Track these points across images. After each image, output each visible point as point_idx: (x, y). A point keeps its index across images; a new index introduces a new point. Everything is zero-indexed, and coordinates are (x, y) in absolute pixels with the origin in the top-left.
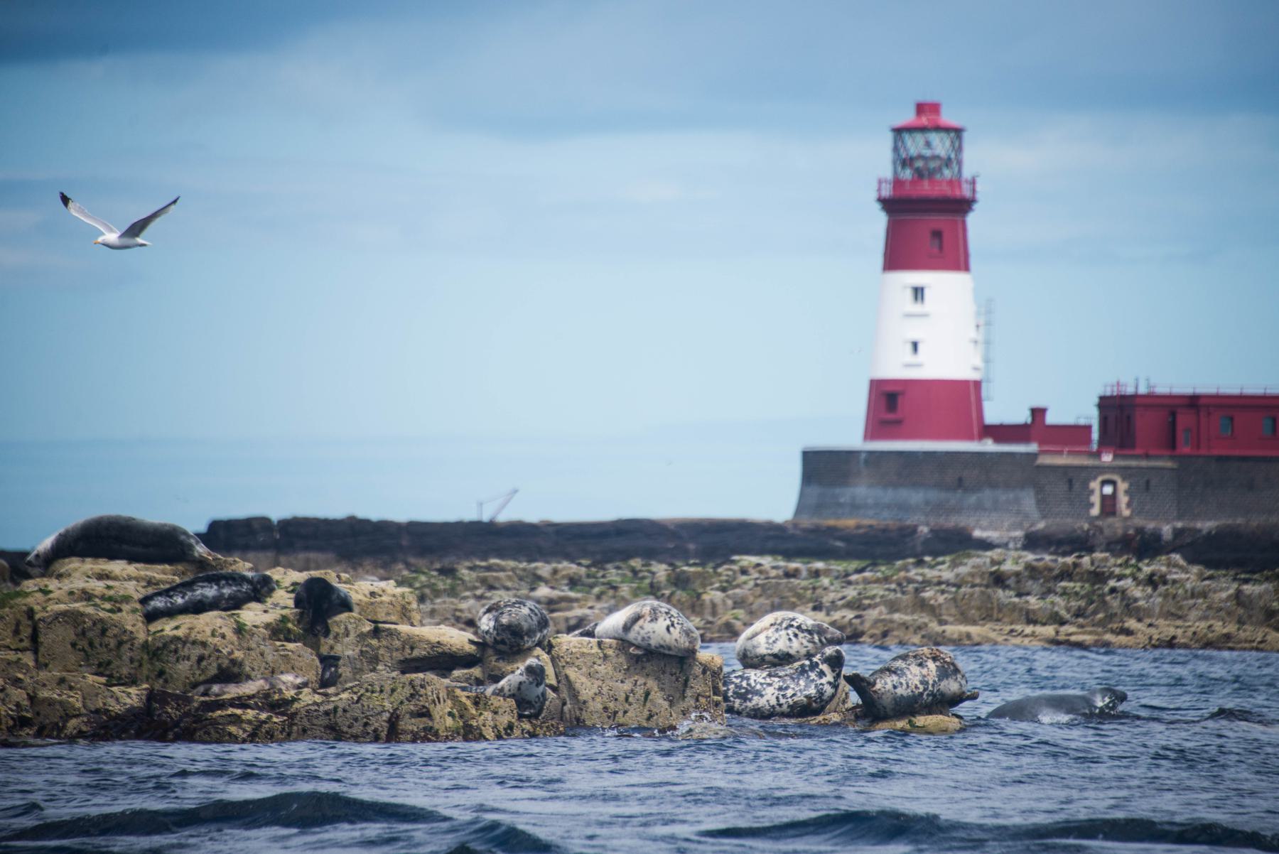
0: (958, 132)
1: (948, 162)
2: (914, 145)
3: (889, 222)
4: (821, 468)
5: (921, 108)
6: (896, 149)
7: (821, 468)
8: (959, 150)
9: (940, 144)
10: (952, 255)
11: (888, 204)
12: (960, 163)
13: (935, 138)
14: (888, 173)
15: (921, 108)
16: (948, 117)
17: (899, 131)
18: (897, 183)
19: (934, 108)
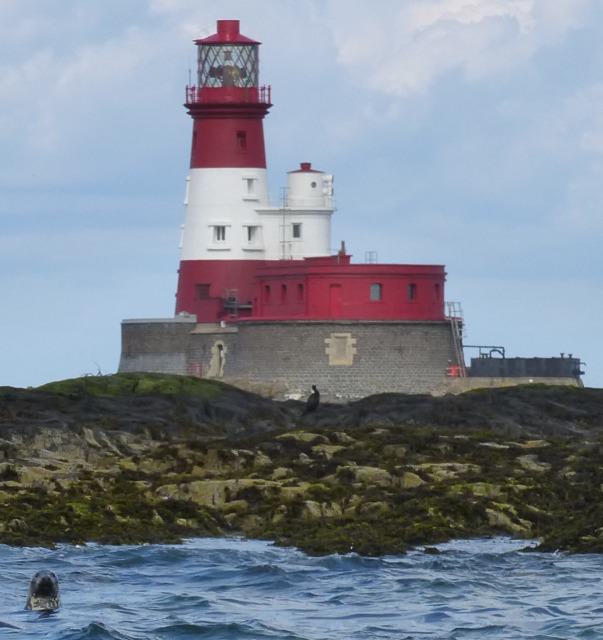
0: (254, 45)
1: (243, 73)
2: (218, 57)
3: (195, 124)
4: (136, 335)
5: (222, 25)
6: (202, 61)
7: (136, 335)
8: (255, 62)
9: (236, 57)
10: (251, 152)
11: (194, 109)
12: (255, 70)
13: (235, 51)
14: (195, 82)
15: (222, 25)
16: (245, 31)
17: (200, 43)
18: (205, 91)
19: (235, 24)
